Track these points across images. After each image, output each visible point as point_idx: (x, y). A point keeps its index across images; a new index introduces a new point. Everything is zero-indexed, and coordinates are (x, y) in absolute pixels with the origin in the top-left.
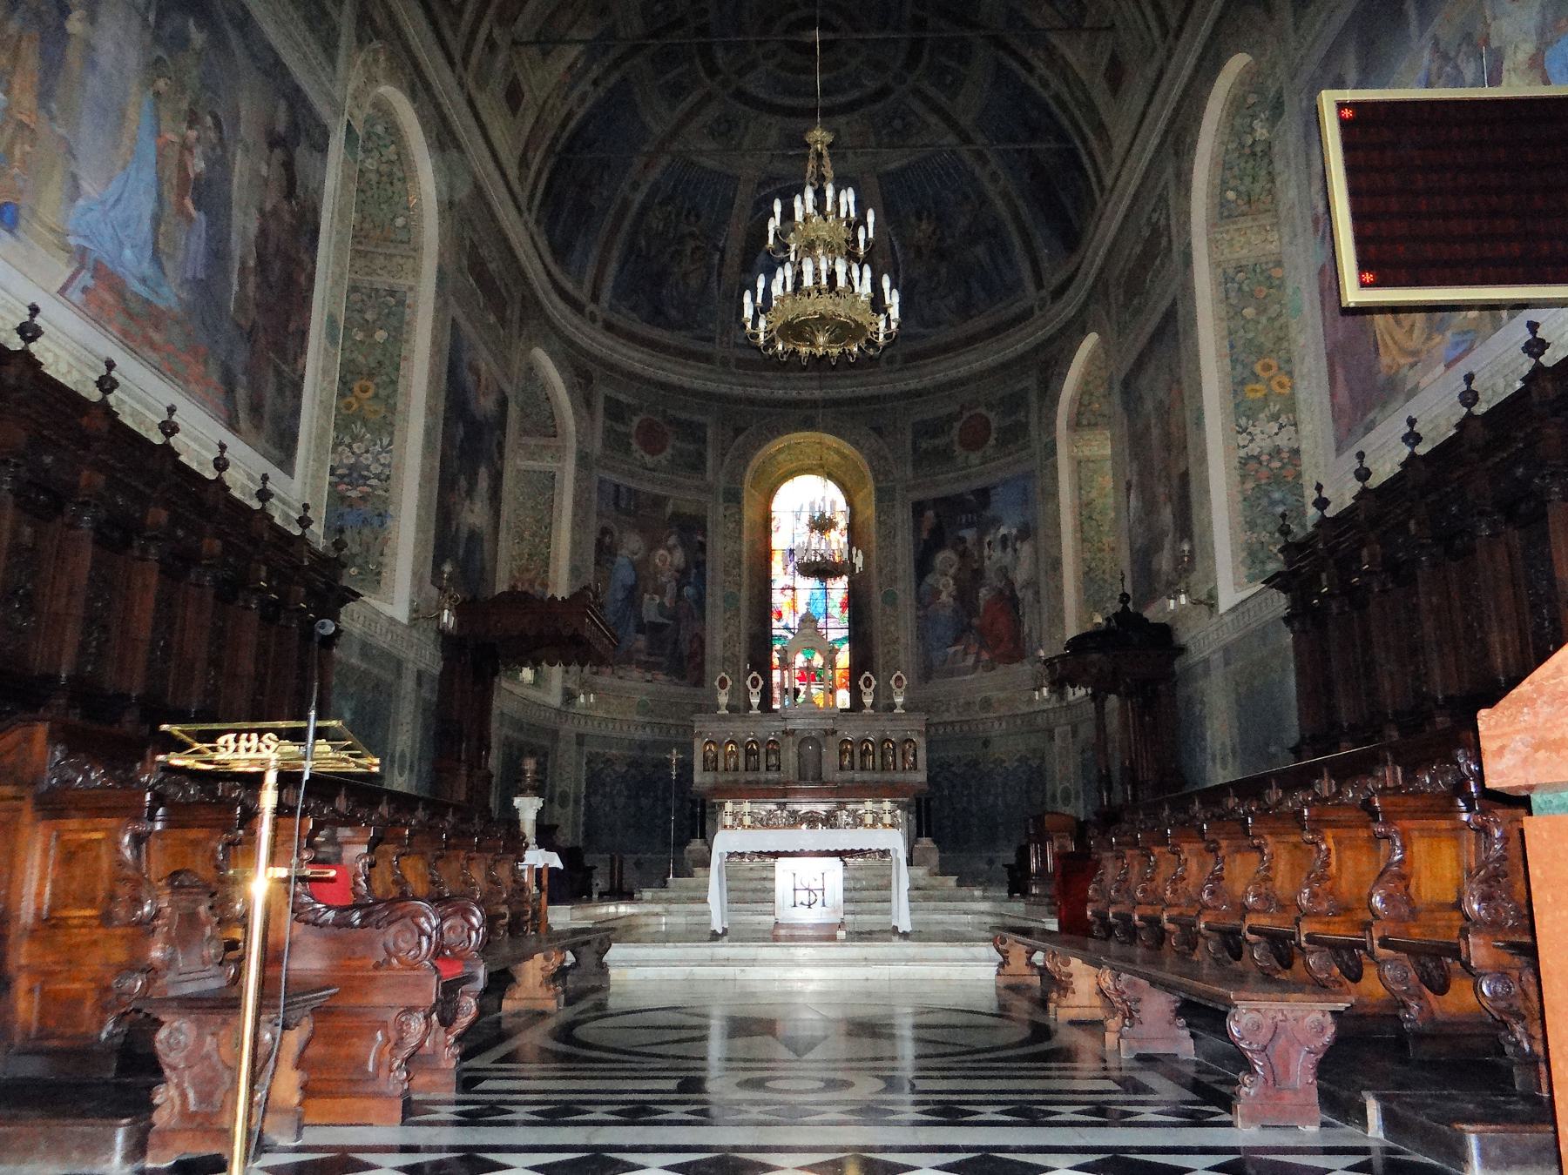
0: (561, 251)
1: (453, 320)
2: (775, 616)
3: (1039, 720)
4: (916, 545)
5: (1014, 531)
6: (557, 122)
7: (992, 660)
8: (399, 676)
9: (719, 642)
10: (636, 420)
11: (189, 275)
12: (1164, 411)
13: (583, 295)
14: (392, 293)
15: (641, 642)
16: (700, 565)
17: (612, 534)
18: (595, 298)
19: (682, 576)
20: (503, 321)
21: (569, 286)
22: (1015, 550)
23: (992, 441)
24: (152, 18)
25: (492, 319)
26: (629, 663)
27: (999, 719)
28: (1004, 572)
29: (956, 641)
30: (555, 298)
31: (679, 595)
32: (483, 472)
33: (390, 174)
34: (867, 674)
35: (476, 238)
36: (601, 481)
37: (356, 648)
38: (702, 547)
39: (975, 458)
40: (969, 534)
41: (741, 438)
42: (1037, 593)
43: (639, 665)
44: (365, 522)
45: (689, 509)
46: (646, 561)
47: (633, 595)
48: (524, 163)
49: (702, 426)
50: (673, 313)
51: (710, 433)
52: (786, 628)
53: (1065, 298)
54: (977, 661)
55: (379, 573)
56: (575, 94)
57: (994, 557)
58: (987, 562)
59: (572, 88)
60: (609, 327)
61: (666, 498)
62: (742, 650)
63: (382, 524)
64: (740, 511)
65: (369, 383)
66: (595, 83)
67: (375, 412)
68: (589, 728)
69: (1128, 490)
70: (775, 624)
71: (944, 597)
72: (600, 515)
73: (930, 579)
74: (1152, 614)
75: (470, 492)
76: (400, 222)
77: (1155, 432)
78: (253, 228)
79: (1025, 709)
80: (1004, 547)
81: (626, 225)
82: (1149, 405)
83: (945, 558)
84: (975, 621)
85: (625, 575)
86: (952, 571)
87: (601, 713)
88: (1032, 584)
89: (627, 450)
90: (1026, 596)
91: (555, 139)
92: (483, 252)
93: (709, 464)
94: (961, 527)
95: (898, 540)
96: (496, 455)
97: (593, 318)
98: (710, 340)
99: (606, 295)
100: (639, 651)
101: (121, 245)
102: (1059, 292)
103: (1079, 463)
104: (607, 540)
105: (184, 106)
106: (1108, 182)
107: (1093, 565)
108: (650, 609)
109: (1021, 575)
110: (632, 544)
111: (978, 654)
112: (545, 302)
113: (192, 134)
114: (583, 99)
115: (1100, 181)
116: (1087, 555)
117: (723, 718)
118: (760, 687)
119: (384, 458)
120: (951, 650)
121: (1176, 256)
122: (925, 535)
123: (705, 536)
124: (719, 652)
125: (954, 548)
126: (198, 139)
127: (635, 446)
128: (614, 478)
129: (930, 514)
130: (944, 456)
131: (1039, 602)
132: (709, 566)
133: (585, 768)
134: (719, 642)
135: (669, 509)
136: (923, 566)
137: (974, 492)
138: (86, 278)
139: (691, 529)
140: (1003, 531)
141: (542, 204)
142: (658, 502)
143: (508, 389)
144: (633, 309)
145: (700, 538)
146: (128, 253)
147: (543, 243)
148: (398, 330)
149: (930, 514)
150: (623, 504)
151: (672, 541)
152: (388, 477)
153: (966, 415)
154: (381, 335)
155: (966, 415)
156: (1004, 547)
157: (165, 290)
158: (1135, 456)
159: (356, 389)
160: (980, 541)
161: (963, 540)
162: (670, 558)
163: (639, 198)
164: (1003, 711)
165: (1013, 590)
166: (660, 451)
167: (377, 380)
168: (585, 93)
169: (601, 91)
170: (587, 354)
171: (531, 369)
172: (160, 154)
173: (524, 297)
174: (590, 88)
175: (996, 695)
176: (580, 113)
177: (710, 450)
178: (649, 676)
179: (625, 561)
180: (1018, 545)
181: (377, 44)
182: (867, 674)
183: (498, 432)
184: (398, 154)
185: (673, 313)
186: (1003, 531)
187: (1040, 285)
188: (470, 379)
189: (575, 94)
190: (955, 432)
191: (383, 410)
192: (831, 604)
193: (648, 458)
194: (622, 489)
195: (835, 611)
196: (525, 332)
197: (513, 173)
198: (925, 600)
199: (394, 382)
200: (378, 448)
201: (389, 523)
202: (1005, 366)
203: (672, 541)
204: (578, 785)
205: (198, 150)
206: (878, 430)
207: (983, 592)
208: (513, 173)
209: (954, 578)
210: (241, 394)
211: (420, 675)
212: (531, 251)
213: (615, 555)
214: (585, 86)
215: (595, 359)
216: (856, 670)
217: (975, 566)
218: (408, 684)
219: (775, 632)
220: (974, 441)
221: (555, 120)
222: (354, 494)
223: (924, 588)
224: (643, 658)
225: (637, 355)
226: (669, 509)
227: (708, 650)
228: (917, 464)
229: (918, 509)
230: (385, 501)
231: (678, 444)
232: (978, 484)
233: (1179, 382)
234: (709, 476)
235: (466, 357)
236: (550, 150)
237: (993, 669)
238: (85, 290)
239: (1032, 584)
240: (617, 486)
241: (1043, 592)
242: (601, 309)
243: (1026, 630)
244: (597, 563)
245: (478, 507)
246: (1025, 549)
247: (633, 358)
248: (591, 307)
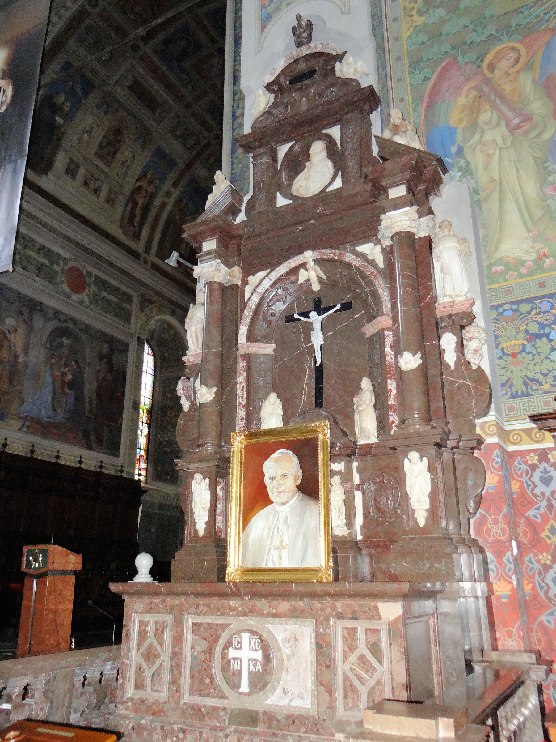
11: (68, 410)
24: (48, 345)
33: (174, 339)
78: (94, 386)
101: (40, 410)
105: (62, 363)
113: (66, 370)
126: (69, 370)
138: (28, 423)
146: (43, 411)
157: (58, 418)
167: (175, 409)
172: (53, 380)
181: (153, 305)
184: (175, 332)
205: (69, 373)
210: (92, 438)
222: (168, 450)
238: (28, 427)
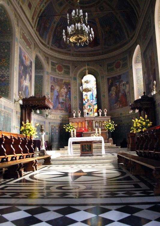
0: (42, 35)
1: (20, 48)
2: (84, 100)
3: (130, 116)
4: (108, 86)
5: (125, 83)
6: (39, 11)
7: (122, 106)
8: (12, 112)
9: (73, 105)
10: (57, 66)
12: (150, 57)
13: (46, 43)
14: (8, 43)
15: (60, 105)
16: (70, 91)
17: (53, 86)
18: (48, 44)
19: (66, 94)
20: (30, 48)
21: (44, 42)
22: (125, 86)
23: (121, 66)
25: (28, 47)
26: (57, 109)
27: (124, 116)
28: (124, 90)
29: (116, 103)
30: (40, 44)
31: (66, 97)
32: (28, 75)
33: (6, 21)
34: (100, 109)
35: (24, 32)
36: (51, 77)
37: (3, 107)
38: (70, 88)
39: (118, 70)
40: (117, 84)
41: (76, 68)
42: (130, 94)
43: (59, 109)
44: (5, 85)
45: (68, 81)
46: (60, 91)
47: (58, 97)
48: (33, 19)
49: (69, 66)
50: (63, 46)
51: (70, 67)
52: (86, 102)
53: (133, 39)
54: (119, 106)
55: (8, 94)
56: (42, 5)
57: (122, 88)
58: (121, 88)
59: (41, 4)
60: (51, 49)
61: (63, 80)
62: (78, 106)
63: (8, 85)
64: (76, 81)
65: (4, 59)
66: (45, 3)
67: (6, 65)
68: (51, 121)
69: (145, 73)
70: (84, 101)
71: (113, 95)
72: (51, 83)
73: (111, 92)
74: (149, 96)
75: (25, 79)
76: (8, 29)
77: (149, 62)
79: (128, 115)
80: (124, 86)
81: (53, 30)
82: (148, 57)
83: (113, 88)
84: (119, 99)
85: (56, 94)
86: (115, 90)
87: (53, 118)
88: (129, 92)
89: (56, 71)
90: (127, 94)
91: (39, 14)
92: (25, 35)
93: (70, 73)
94: (116, 82)
95: (105, 85)
96: (30, 72)
97: (48, 47)
98: (70, 51)
99: (50, 43)
100: (59, 107)
102: (132, 38)
103: (137, 69)
104: (53, 87)
106: (140, 16)
107: (140, 88)
108: (61, 100)
109: (127, 90)
110: (57, 88)
111: (120, 105)
112: (39, 45)
114: (43, 7)
115: (138, 15)
116: (138, 86)
117: (74, 119)
118: (80, 113)
119: (8, 73)
120: (115, 105)
121: (152, 28)
122: (110, 84)
123: (70, 86)
124: (73, 107)
125: (115, 86)
127: (57, 70)
128: (54, 76)
129: (110, 80)
130: (112, 69)
131: (130, 95)
132: (71, 91)
133: (50, 128)
134: (73, 105)
135: (64, 81)
136: (109, 90)
137: (118, 76)
139: (68, 85)
140: (123, 83)
141: (37, 26)
142: (62, 80)
143: (32, 60)
144: (56, 45)
145: (69, 86)
147: (38, 33)
148: (9, 49)
149: (110, 80)
150: (55, 81)
151: (64, 87)
152: (9, 76)
153: (116, 62)
154: (6, 51)
155: (116, 62)
156: (124, 86)
158: (146, 67)
159: (2, 60)
160: (119, 84)
161: (116, 85)
162: (64, 90)
163: (55, 25)
164: (124, 115)
165: (125, 94)
166: (61, 71)
168: (44, 5)
169: (47, 5)
170: (47, 54)
171: (37, 57)
173: (34, 43)
174: (44, 4)
175: (122, 112)
176: (43, 9)
177: (70, 71)
178: (61, 111)
179: (56, 91)
180: (126, 85)
182: (100, 109)
183: (30, 68)
184: (7, 16)
185: (63, 46)
186: (123, 83)
187: (128, 37)
188: (24, 58)
189: (42, 5)
190: (114, 66)
191: (7, 64)
192: (93, 97)
193: (59, 73)
194: (55, 78)
195: (94, 99)
196: (35, 50)
197: (31, 21)
198: (110, 96)
199: (9, 59)
200: (7, 71)
201: (9, 85)
202: (123, 52)
203: (64, 87)
204: (49, 131)
206: (101, 66)
207: (120, 94)
208: (31, 21)
209: (115, 92)
211: (17, 112)
212: (35, 35)
213: (54, 90)
214: (43, 4)
215: (49, 55)
216: (98, 109)
217: (119, 89)
218: (14, 114)
219: (84, 103)
220: (118, 66)
221: (38, 11)
222: (3, 80)
223: (109, 94)
224: (60, 108)
225: (57, 54)
226: (64, 81)
227: (72, 107)
228: (108, 71)
229: (108, 79)
230: (9, 81)
231: (65, 70)
232: (118, 74)
233: (153, 52)
234: (71, 75)
235: (23, 54)
236: (38, 16)
237: (122, 108)
239: (129, 92)
240: (54, 78)
241: (131, 93)
242: (50, 46)
243: (128, 101)
244: (51, 92)
245: (27, 81)
246: (127, 86)
247: (57, 55)
248: (48, 45)
